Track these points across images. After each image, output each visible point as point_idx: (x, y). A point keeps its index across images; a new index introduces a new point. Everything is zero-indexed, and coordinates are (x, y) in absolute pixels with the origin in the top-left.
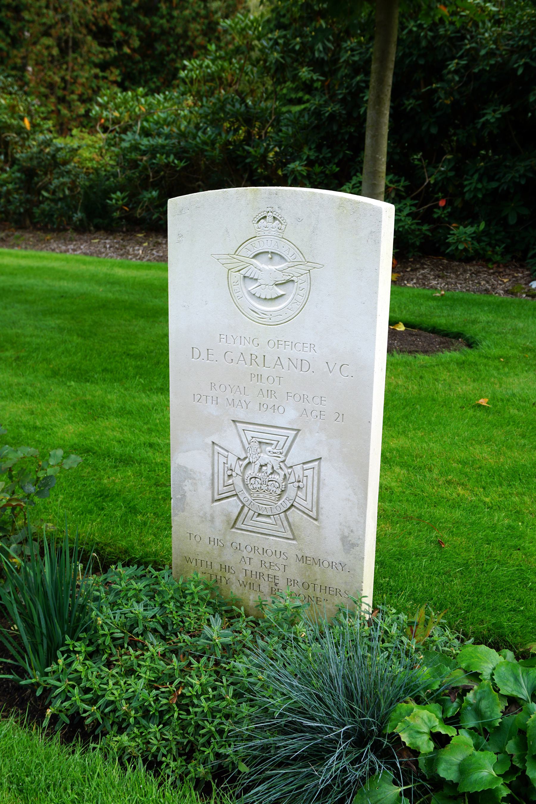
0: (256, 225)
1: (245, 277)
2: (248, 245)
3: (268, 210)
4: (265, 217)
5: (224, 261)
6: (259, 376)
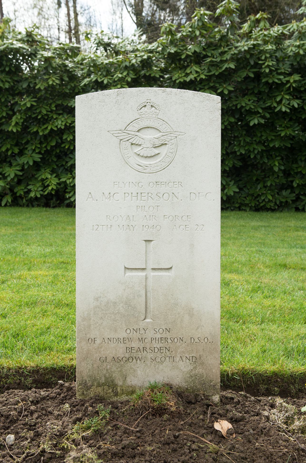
0: (139, 111)
1: (132, 144)
2: (134, 124)
3: (147, 101)
4: (146, 106)
5: (116, 135)
6: (143, 207)
